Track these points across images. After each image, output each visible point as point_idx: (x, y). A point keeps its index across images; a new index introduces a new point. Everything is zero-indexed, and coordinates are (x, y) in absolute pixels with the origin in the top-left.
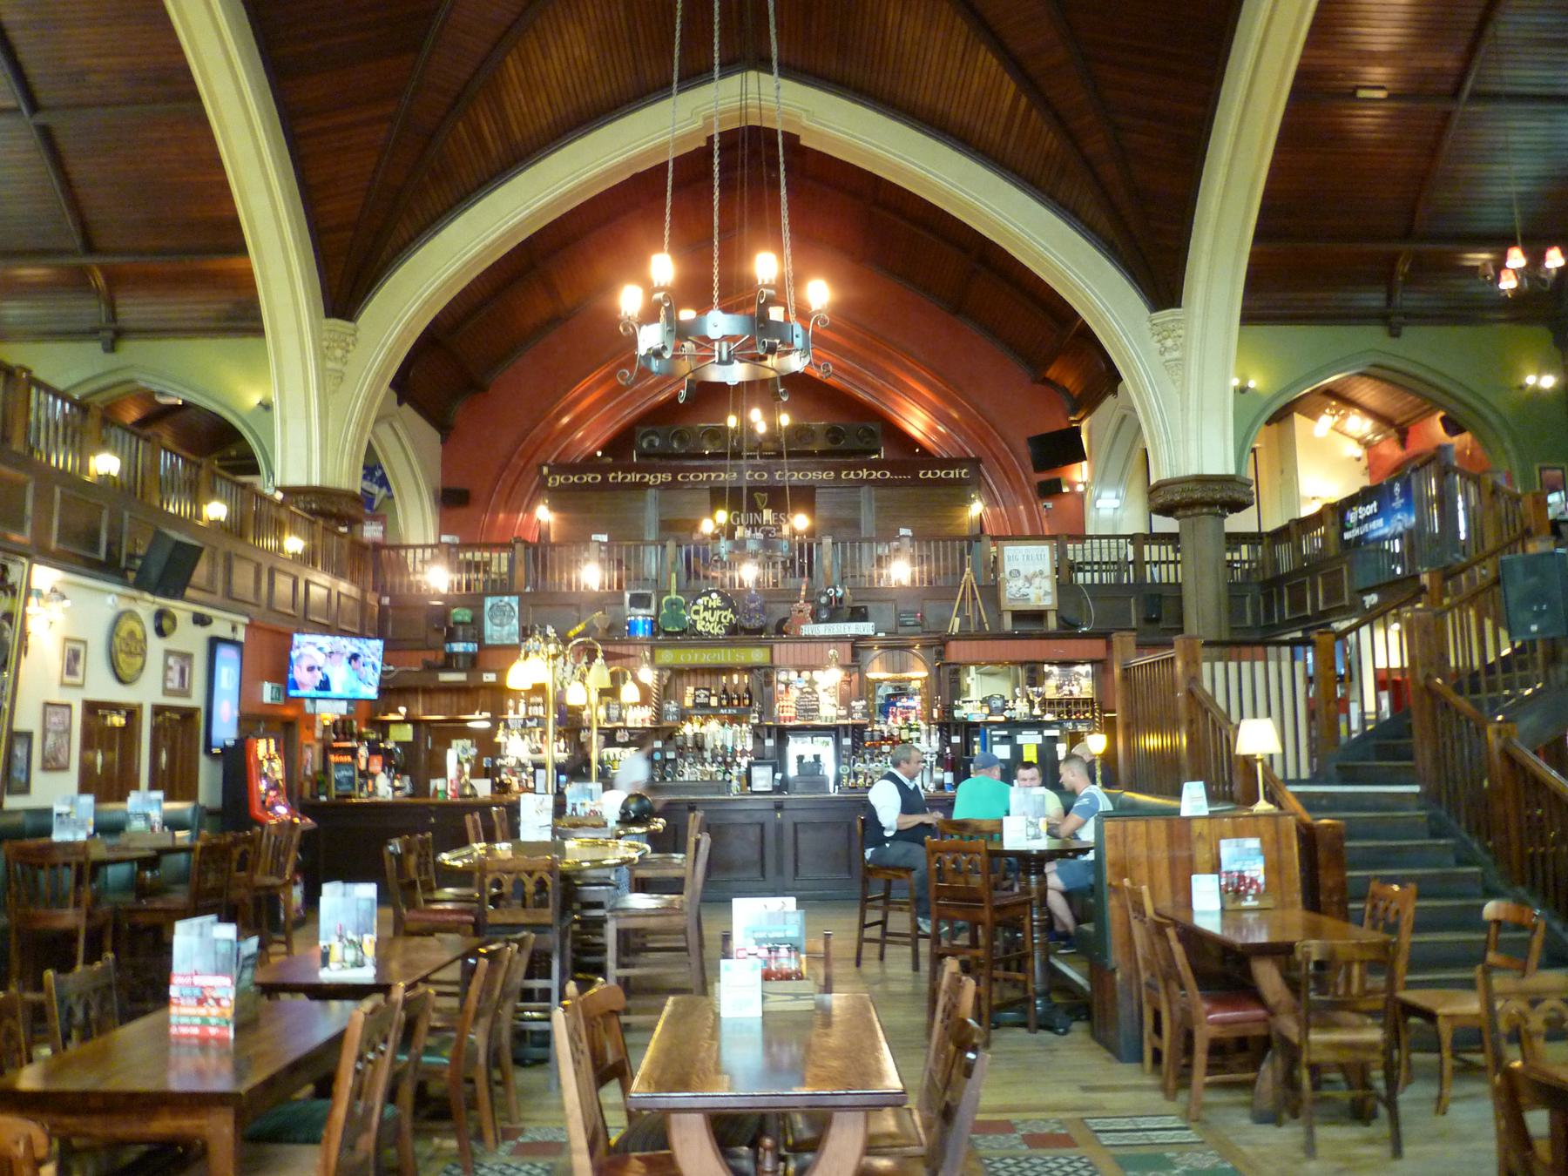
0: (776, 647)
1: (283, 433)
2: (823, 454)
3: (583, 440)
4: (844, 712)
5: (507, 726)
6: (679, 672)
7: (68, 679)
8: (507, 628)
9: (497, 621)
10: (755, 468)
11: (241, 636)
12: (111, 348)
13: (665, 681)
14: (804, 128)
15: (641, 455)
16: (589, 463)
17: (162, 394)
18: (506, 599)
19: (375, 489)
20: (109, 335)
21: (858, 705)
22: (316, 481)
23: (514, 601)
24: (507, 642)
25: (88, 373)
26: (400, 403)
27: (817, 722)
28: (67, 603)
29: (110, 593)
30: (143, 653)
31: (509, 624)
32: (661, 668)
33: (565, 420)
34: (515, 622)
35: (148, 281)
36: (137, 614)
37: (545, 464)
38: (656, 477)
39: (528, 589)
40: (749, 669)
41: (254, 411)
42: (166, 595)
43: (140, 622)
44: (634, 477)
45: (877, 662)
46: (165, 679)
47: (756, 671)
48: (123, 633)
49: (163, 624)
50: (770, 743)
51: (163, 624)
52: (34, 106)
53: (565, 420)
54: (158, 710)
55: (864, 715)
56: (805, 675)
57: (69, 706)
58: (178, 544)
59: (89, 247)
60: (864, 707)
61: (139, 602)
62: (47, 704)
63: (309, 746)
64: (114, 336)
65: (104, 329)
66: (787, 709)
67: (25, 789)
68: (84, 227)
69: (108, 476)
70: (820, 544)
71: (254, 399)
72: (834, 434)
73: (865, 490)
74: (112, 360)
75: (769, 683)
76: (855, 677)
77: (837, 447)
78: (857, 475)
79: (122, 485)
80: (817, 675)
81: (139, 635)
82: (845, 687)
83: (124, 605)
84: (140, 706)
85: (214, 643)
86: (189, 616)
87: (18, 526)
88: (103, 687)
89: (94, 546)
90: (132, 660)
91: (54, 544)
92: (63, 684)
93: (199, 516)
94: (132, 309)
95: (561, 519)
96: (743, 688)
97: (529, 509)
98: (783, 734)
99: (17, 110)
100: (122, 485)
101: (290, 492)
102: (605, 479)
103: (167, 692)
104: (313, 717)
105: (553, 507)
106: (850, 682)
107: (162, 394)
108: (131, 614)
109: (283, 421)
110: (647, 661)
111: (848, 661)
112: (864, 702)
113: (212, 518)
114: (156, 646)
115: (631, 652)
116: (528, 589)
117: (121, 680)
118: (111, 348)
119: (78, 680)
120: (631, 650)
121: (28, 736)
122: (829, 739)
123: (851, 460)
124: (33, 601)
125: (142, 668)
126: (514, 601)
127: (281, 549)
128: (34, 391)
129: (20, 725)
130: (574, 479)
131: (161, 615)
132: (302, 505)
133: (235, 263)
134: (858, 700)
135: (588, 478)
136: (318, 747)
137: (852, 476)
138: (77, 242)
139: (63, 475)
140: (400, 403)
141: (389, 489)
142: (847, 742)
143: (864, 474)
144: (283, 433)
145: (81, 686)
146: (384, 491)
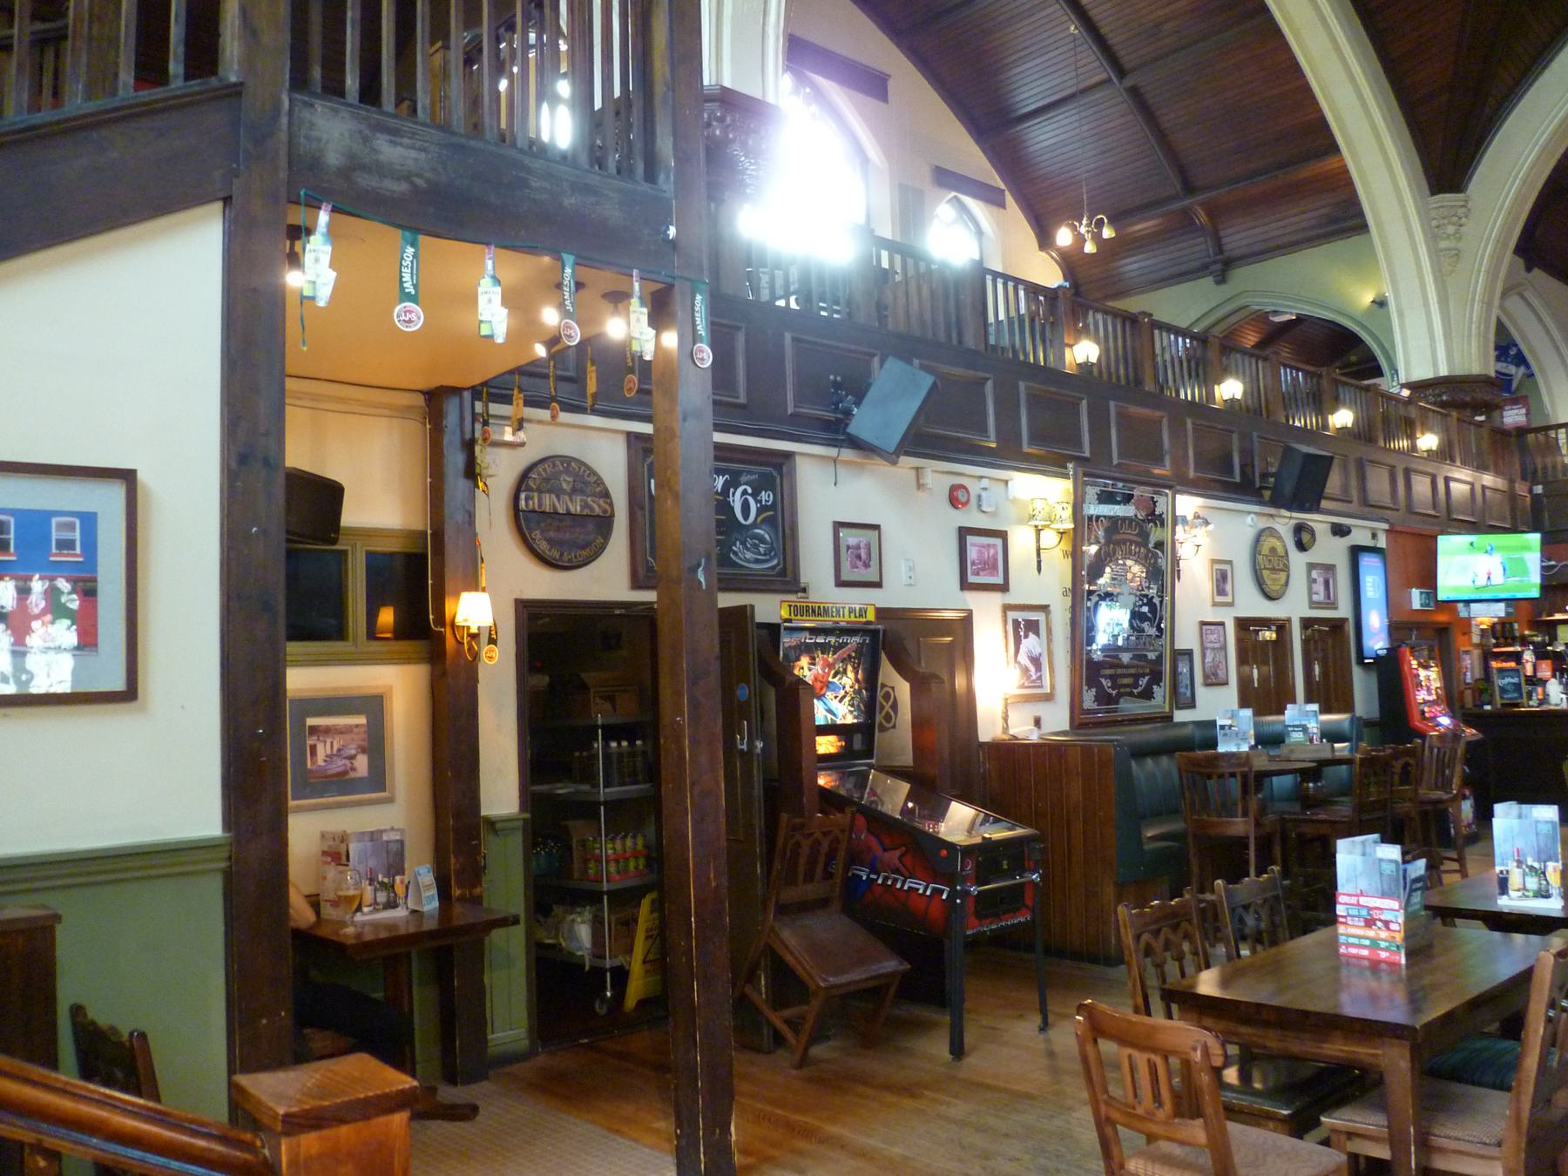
1: (1402, 327)
7: (1219, 599)
11: (1382, 542)
12: (1221, 279)
17: (1275, 313)
19: (1512, 369)
20: (1218, 266)
22: (1443, 371)
25: (1206, 308)
26: (1529, 269)
28: (1211, 527)
29: (1250, 513)
30: (1286, 568)
35: (1248, 206)
41: (1369, 309)
42: (1302, 509)
43: (1280, 538)
46: (1310, 592)
48: (1265, 550)
52: (1122, 73)
54: (1307, 623)
57: (1222, 624)
59: (1189, 188)
61: (1277, 519)
62: (1203, 623)
63: (1467, 652)
64: (1222, 266)
67: (1191, 704)
68: (1182, 171)
69: (1233, 400)
71: (1367, 298)
79: (1247, 408)
81: (1280, 551)
83: (1263, 523)
84: (1289, 620)
85: (1356, 552)
87: (1159, 460)
88: (1252, 605)
89: (1229, 469)
91: (1192, 474)
92: (1215, 604)
93: (1325, 426)
94: (1237, 237)
99: (1109, 80)
100: (1247, 408)
101: (1417, 387)
103: (1313, 605)
104: (1467, 622)
107: (1275, 313)
109: (1401, 315)
113: (1338, 426)
114: (1298, 560)
118: (1221, 279)
119: (1228, 599)
124: (1179, 528)
127: (1414, 448)
128: (1156, 332)
129: (1180, 644)
131: (1299, 529)
132: (1431, 399)
133: (1330, 164)
136: (1476, 653)
139: (1193, 407)
140: (1529, 269)
141: (1528, 366)
144: (1402, 327)
145: (1231, 604)
146: (1522, 370)
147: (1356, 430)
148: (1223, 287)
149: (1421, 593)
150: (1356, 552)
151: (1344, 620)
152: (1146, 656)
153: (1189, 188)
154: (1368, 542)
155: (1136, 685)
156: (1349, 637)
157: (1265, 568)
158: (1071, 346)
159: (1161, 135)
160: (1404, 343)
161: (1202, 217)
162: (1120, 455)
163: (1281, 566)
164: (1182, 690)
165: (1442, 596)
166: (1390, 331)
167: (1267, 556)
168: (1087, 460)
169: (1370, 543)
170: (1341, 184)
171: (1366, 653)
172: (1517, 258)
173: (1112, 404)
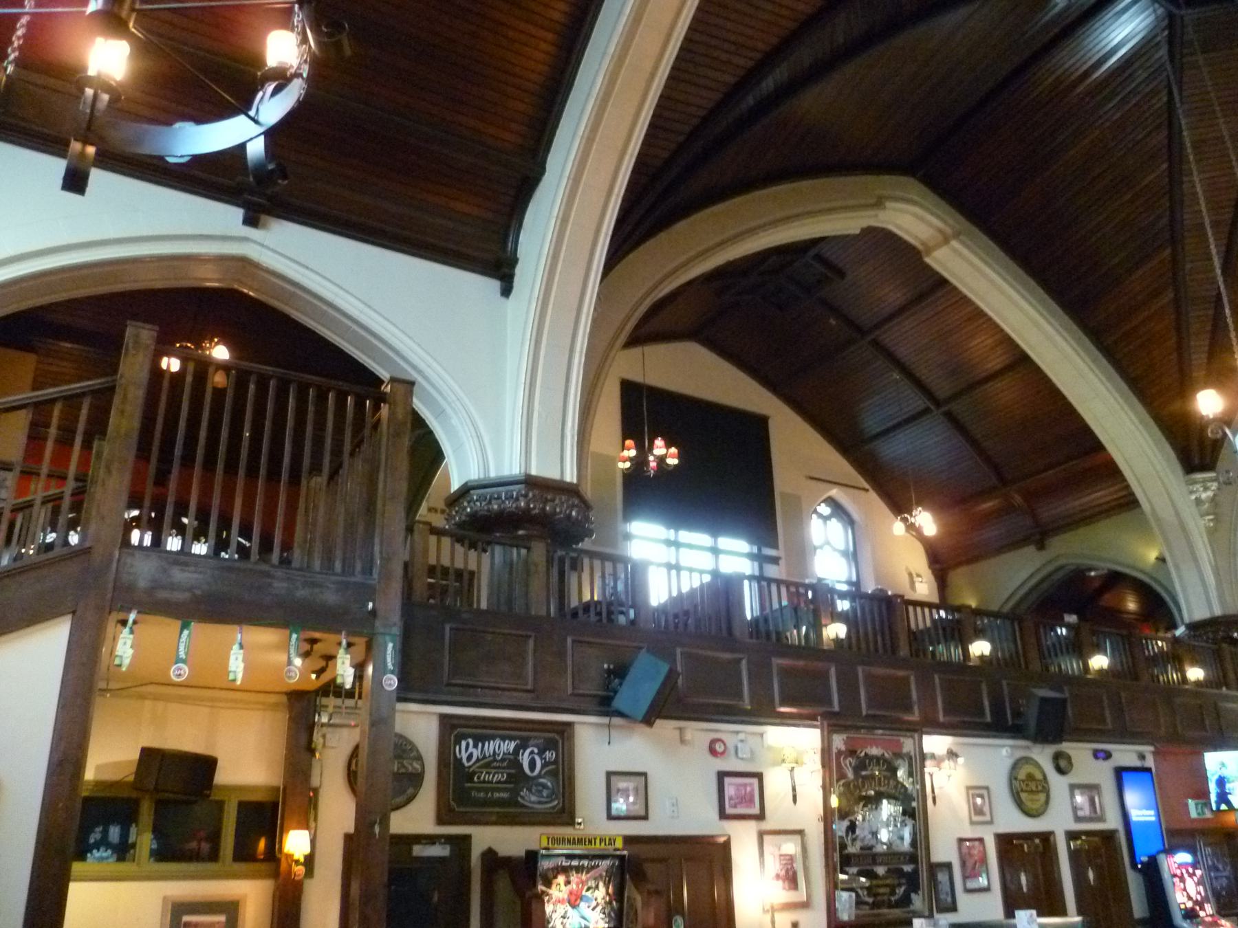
1: (1180, 577)
7: (975, 818)
11: (1150, 762)
12: (1041, 546)
20: (1038, 537)
22: (1218, 612)
25: (1032, 570)
28: (961, 760)
29: (1004, 746)
30: (1046, 790)
36: (1032, 759)
48: (1022, 775)
49: (1062, 765)
51: (1062, 765)
52: (938, 404)
54: (1072, 836)
57: (981, 840)
58: (1044, 700)
59: (1003, 481)
64: (1040, 536)
67: (953, 908)
68: (997, 469)
71: (1152, 555)
79: (1005, 659)
81: (1039, 776)
83: (1020, 754)
84: (1051, 833)
85: (1120, 773)
87: (908, 708)
88: (1016, 823)
90: (1035, 797)
91: (941, 718)
92: (972, 823)
94: (1051, 510)
99: (926, 411)
100: (1005, 659)
101: (1194, 627)
103: (1078, 819)
108: (1027, 760)
109: (1177, 567)
114: (1058, 784)
118: (1041, 546)
119: (988, 818)
121: (948, 866)
125: (1047, 802)
127: (1184, 679)
128: (911, 609)
129: (939, 855)
131: (1057, 757)
132: (1211, 635)
144: (1180, 577)
145: (991, 822)
147: (1119, 668)
148: (1044, 552)
149: (1196, 805)
150: (1120, 773)
152: (902, 869)
153: (1003, 481)
154: (1133, 761)
155: (893, 893)
157: (1022, 790)
158: (826, 626)
160: (1184, 591)
161: (1018, 499)
162: (869, 707)
164: (942, 897)
167: (1023, 781)
168: (835, 714)
169: (1138, 763)
170: (1111, 471)
171: (1138, 860)
173: (860, 669)
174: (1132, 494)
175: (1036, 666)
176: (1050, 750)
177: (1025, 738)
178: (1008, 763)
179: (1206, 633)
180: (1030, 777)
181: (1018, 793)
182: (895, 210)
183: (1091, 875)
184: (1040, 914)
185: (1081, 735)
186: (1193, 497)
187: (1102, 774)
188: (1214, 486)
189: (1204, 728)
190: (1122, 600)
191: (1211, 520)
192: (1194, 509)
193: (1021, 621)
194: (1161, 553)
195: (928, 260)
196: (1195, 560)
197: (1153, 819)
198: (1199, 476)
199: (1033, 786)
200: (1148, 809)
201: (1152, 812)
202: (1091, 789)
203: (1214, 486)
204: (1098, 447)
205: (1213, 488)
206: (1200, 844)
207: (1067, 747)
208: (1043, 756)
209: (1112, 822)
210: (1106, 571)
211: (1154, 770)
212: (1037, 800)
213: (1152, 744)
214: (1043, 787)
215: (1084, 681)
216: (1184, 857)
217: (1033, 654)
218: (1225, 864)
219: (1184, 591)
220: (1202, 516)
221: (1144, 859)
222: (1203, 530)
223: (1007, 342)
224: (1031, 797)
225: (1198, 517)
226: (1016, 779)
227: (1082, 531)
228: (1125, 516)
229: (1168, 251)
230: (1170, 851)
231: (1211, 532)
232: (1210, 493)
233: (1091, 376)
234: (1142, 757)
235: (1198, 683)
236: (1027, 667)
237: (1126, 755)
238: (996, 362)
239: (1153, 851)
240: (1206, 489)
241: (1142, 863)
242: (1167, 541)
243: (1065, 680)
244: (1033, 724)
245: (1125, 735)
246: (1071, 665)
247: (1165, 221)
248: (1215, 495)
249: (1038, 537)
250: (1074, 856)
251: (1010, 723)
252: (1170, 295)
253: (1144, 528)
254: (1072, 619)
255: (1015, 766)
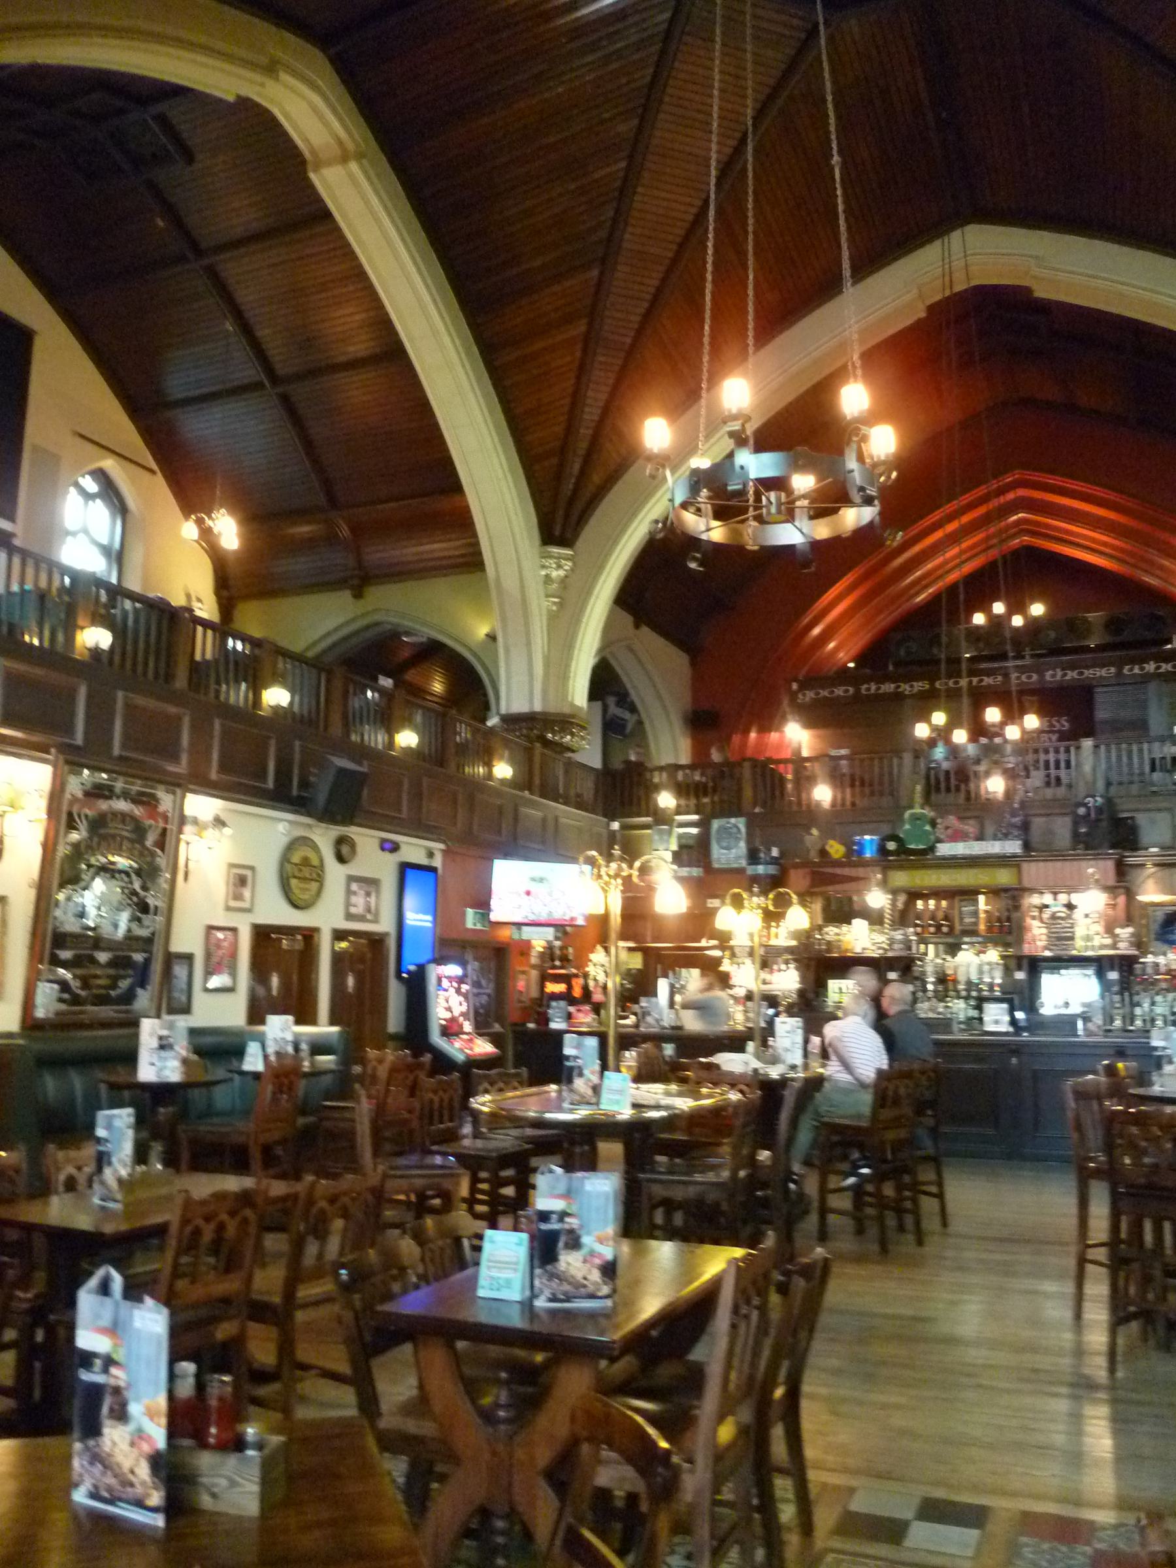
0: (1025, 866)
2: (1101, 648)
3: (837, 649)
4: (1108, 941)
5: (733, 955)
6: (914, 895)
7: (233, 904)
8: (734, 851)
9: (724, 844)
10: (1021, 669)
11: (437, 862)
12: (358, 595)
13: (900, 905)
14: (1034, 277)
15: (896, 665)
16: (843, 676)
17: (407, 634)
18: (733, 820)
19: (627, 715)
20: (355, 582)
21: (1125, 932)
22: (538, 707)
23: (740, 823)
24: (735, 866)
25: (341, 620)
27: (1074, 953)
29: (282, 820)
31: (736, 846)
32: (894, 892)
33: (816, 631)
34: (742, 845)
37: (795, 680)
38: (912, 686)
39: (757, 810)
40: (995, 892)
44: (888, 687)
45: (1150, 885)
46: (348, 904)
47: (1003, 895)
48: (296, 858)
50: (1020, 975)
52: (274, 379)
53: (816, 631)
54: (339, 935)
55: (1132, 944)
56: (1063, 898)
57: (234, 930)
58: (342, 772)
60: (1133, 935)
62: (211, 928)
63: (524, 972)
65: (352, 577)
66: (1037, 937)
67: (186, 1010)
68: (327, 485)
70: (1078, 748)
71: (482, 630)
72: (1113, 625)
73: (1152, 687)
74: (361, 606)
75: (1017, 907)
76: (1122, 900)
77: (1118, 639)
78: (1142, 669)
79: (302, 716)
80: (1075, 898)
81: (315, 862)
82: (1110, 912)
85: (405, 868)
86: (375, 844)
87: (175, 757)
89: (262, 775)
91: (214, 775)
92: (228, 909)
93: (391, 744)
94: (379, 553)
95: (819, 737)
96: (940, 915)
97: (779, 728)
98: (1035, 966)
100: (302, 716)
101: (512, 721)
102: (858, 691)
103: (349, 917)
105: (809, 724)
106: (1114, 906)
107: (407, 634)
108: (305, 841)
109: (507, 651)
110: (878, 885)
111: (1111, 880)
112: (1130, 930)
114: (335, 873)
115: (862, 875)
116: (757, 810)
117: (295, 906)
118: (358, 595)
119: (246, 905)
120: (860, 872)
121: (188, 958)
122: (1090, 972)
123: (1132, 652)
124: (188, 829)
126: (740, 823)
127: (490, 776)
128: (200, 629)
129: (178, 945)
130: (824, 693)
131: (341, 841)
134: (1123, 927)
135: (839, 691)
136: (534, 974)
137: (1136, 670)
138: (322, 500)
139: (230, 713)
140: (637, 626)
142: (1113, 975)
143: (1151, 667)
145: (249, 910)
146: (635, 718)
147: (427, 751)
148: (362, 602)
150: (405, 868)
151: (386, 934)
152: (130, 958)
154: (422, 860)
155: (114, 986)
156: (388, 950)
157: (295, 877)
158: (82, 628)
159: (309, 445)
161: (345, 531)
162: (124, 746)
163: (314, 876)
164: (176, 995)
165: (494, 916)
166: (497, 667)
167: (296, 865)
168: (78, 748)
169: (424, 861)
170: (462, 522)
171: (404, 969)
172: (618, 609)
173: (120, 694)
174: (480, 554)
175: (336, 730)
176: (336, 831)
177: (309, 814)
178: (284, 841)
179: (520, 729)
180: (306, 862)
181: (288, 879)
182: (287, 86)
183: (351, 981)
184: (298, 1022)
185: (373, 821)
186: (543, 573)
187: (384, 868)
188: (568, 565)
189: (499, 832)
190: (429, 679)
191: (555, 603)
192: (541, 587)
193: (329, 672)
194: (493, 630)
195: (312, 176)
196: (528, 644)
197: (429, 925)
198: (556, 550)
199: (306, 872)
200: (425, 913)
201: (430, 918)
202: (371, 884)
203: (568, 565)
204: (455, 487)
205: (567, 568)
206: (469, 956)
207: (353, 831)
208: (324, 837)
209: (385, 925)
210: (424, 640)
211: (440, 871)
212: (307, 890)
213: (444, 842)
214: (319, 875)
215: (383, 759)
216: (454, 970)
217: (336, 718)
218: (489, 980)
219: (509, 678)
220: (547, 596)
221: (412, 968)
222: (544, 612)
223: (383, 325)
224: (302, 885)
225: (542, 594)
226: (289, 862)
227: (410, 585)
228: (464, 579)
229: (595, 273)
230: (440, 960)
231: (553, 618)
232: (561, 573)
233: (471, 396)
234: (431, 855)
235: (503, 781)
236: (326, 728)
237: (414, 850)
238: (360, 347)
239: (422, 960)
240: (559, 567)
241: (409, 972)
242: (504, 620)
243: (363, 753)
244: (322, 797)
245: (420, 828)
246: (378, 739)
247: (603, 234)
248: (566, 576)
249: (355, 582)
250: (338, 959)
251: (295, 792)
252: (581, 327)
253: (482, 598)
254: (386, 682)
255: (291, 847)
